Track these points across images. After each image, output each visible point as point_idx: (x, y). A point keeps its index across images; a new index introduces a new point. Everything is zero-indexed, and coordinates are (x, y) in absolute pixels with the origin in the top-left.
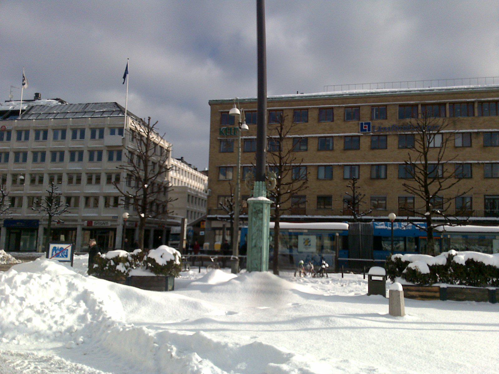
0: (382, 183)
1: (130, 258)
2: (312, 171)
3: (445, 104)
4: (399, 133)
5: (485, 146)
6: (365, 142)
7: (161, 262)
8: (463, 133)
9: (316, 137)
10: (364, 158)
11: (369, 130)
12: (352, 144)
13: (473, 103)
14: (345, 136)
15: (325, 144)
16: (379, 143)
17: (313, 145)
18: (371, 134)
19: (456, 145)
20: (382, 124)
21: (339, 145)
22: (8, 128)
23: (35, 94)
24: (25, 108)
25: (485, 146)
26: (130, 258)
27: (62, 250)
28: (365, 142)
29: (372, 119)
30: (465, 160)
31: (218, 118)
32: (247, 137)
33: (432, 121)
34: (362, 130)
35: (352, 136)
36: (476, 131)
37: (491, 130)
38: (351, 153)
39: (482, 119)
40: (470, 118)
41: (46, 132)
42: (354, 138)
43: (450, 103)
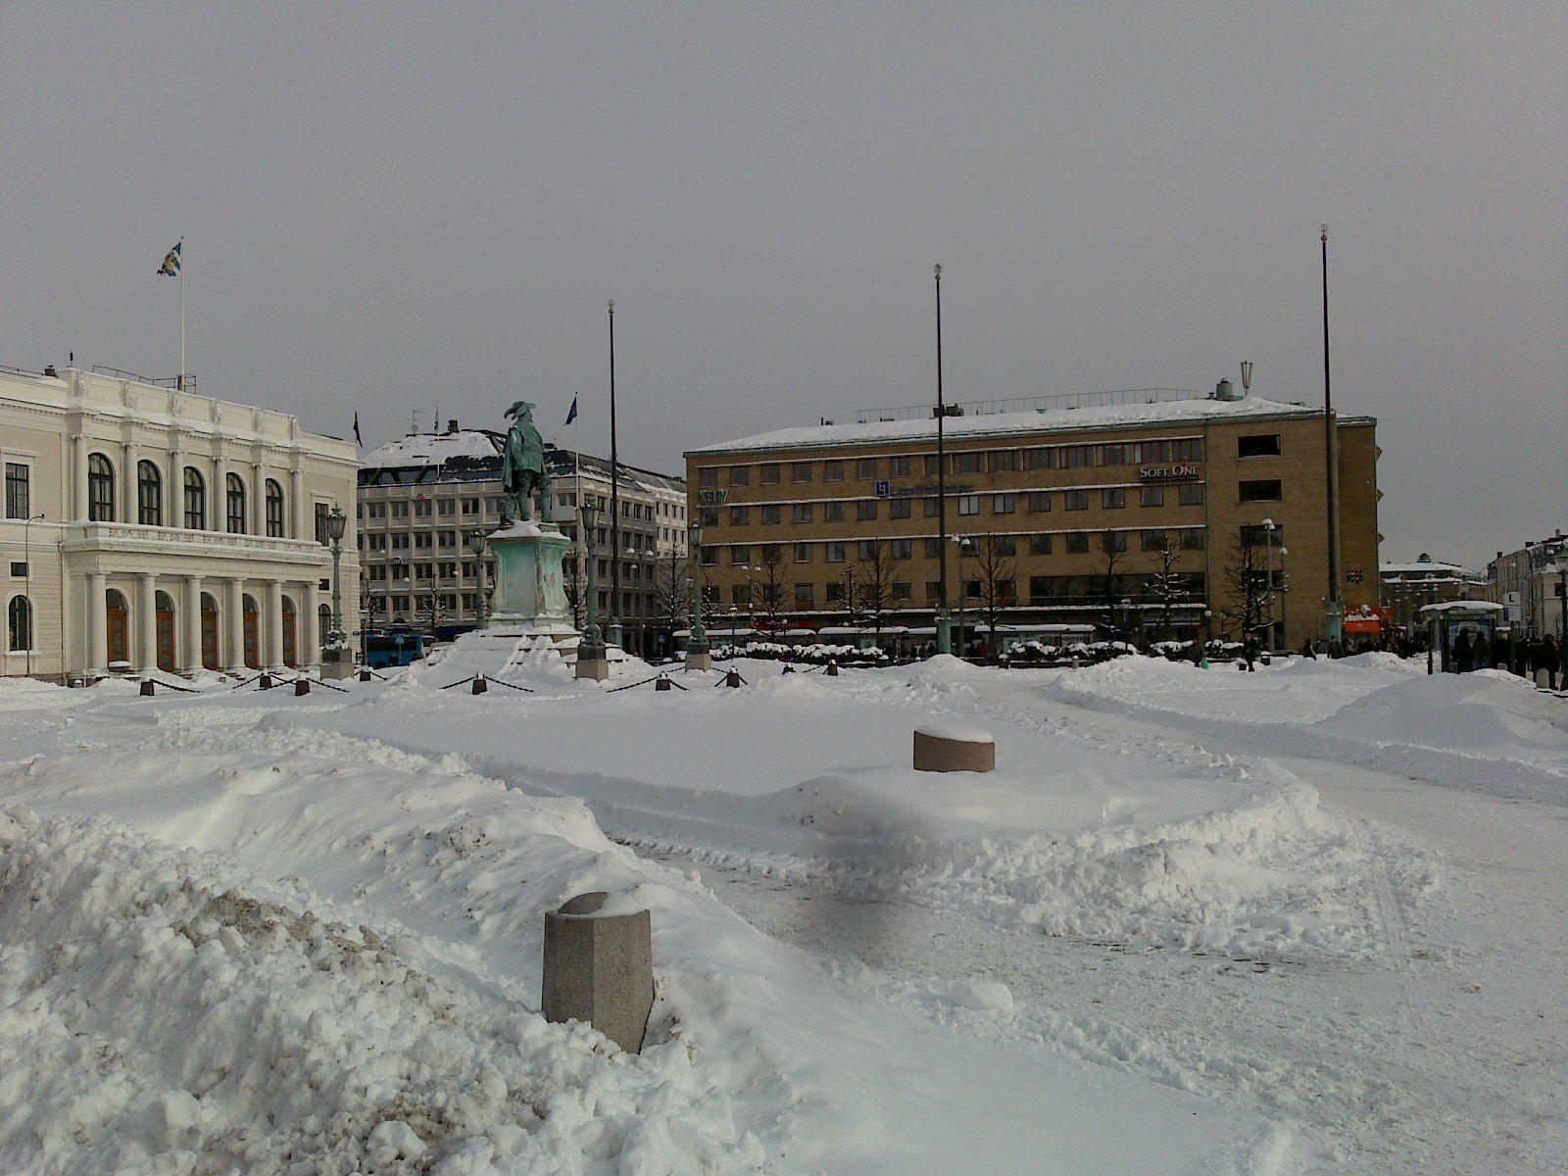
0: (905, 564)
2: (819, 552)
3: (983, 452)
4: (924, 496)
5: (1031, 512)
6: (883, 510)
8: (1003, 494)
9: (821, 503)
10: (885, 531)
11: (887, 492)
12: (866, 511)
13: (1017, 450)
14: (858, 502)
15: (835, 511)
16: (900, 512)
17: (818, 514)
18: (891, 497)
19: (997, 510)
20: (904, 483)
21: (851, 513)
23: (450, 422)
24: (443, 462)
25: (1031, 512)
28: (883, 510)
29: (891, 477)
30: (1006, 531)
31: (697, 478)
32: (734, 504)
33: (966, 478)
34: (878, 491)
35: (867, 501)
36: (1018, 491)
37: (1037, 490)
38: (867, 524)
39: (1026, 474)
40: (1013, 473)
41: (476, 503)
42: (861, 504)
43: (989, 452)
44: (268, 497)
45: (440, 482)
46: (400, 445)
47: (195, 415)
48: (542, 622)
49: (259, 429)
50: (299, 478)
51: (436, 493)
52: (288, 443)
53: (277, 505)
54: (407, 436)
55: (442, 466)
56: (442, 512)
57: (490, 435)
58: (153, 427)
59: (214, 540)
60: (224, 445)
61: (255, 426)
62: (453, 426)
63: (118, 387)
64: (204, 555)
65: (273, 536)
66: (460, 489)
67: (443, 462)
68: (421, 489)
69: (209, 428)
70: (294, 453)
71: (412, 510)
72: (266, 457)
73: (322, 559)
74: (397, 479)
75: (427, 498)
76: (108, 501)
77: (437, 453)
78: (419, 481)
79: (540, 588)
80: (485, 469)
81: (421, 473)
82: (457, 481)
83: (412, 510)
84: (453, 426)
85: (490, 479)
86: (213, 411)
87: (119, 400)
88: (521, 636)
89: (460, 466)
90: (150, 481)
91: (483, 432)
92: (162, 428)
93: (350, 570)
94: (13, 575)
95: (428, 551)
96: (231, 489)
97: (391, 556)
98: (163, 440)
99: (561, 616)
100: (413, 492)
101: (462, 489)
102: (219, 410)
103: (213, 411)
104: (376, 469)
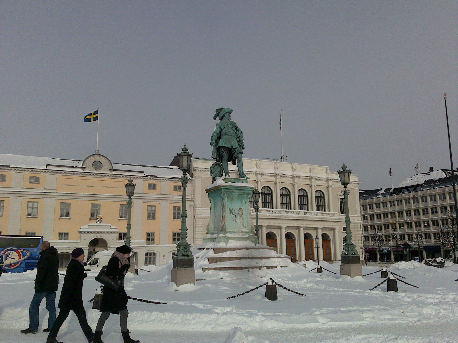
1: (432, 261)
7: (438, 261)
22: (416, 196)
26: (432, 261)
27: (417, 258)
44: (298, 195)
45: (421, 190)
46: (411, 179)
47: (285, 169)
48: (221, 240)
49: (311, 172)
50: (330, 189)
51: (420, 194)
52: (325, 176)
53: (323, 200)
54: (415, 175)
55: (422, 184)
56: (423, 201)
57: (444, 171)
58: (303, 178)
59: (295, 213)
60: (313, 180)
61: (275, 168)
62: (431, 169)
63: (255, 162)
64: (285, 218)
65: (304, 210)
66: (428, 192)
67: (423, 182)
68: (415, 193)
69: (290, 173)
70: (327, 180)
71: (412, 201)
72: (314, 182)
73: (338, 219)
74: (408, 190)
75: (417, 196)
76: (323, 205)
77: (420, 180)
78: (414, 191)
79: (223, 218)
80: (438, 183)
81: (415, 188)
82: (427, 189)
83: (412, 201)
84: (431, 169)
85: (440, 187)
86: (292, 167)
87: (255, 166)
88: (204, 249)
89: (429, 183)
90: (303, 196)
91: (442, 170)
92: (307, 178)
93: (356, 223)
94: (343, 231)
95: (427, 216)
96: (299, 194)
97: (405, 219)
98: (325, 183)
99: (247, 236)
100: (412, 194)
101: (429, 192)
102: (294, 167)
103: (292, 167)
104: (400, 188)
